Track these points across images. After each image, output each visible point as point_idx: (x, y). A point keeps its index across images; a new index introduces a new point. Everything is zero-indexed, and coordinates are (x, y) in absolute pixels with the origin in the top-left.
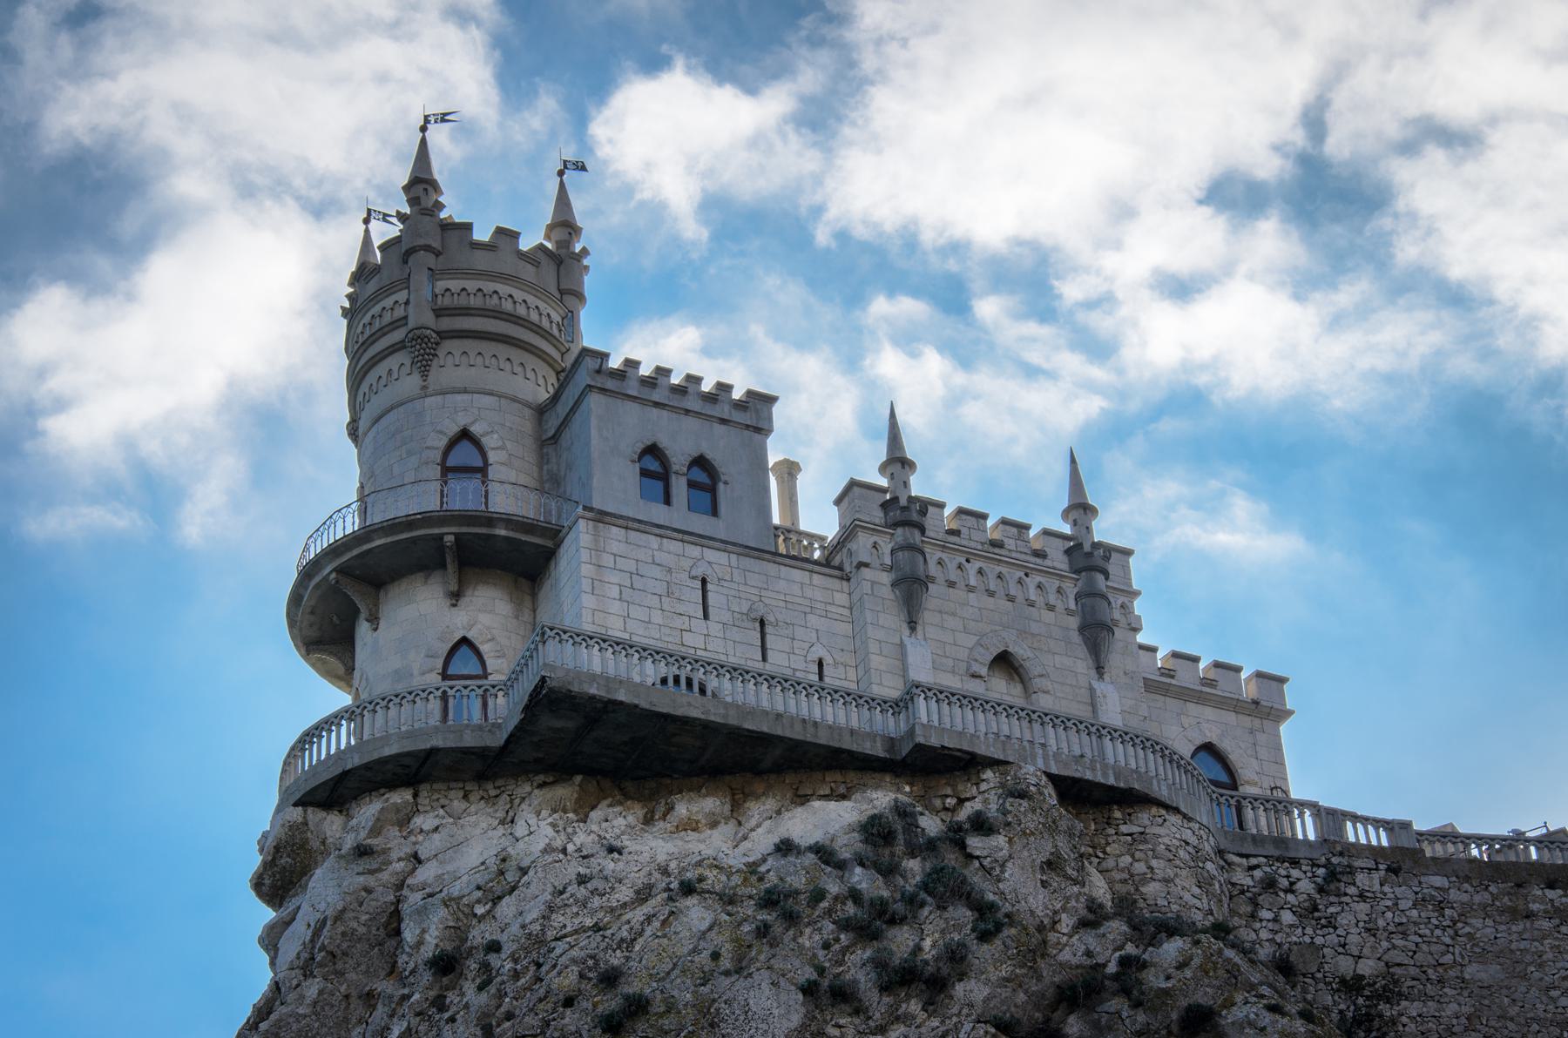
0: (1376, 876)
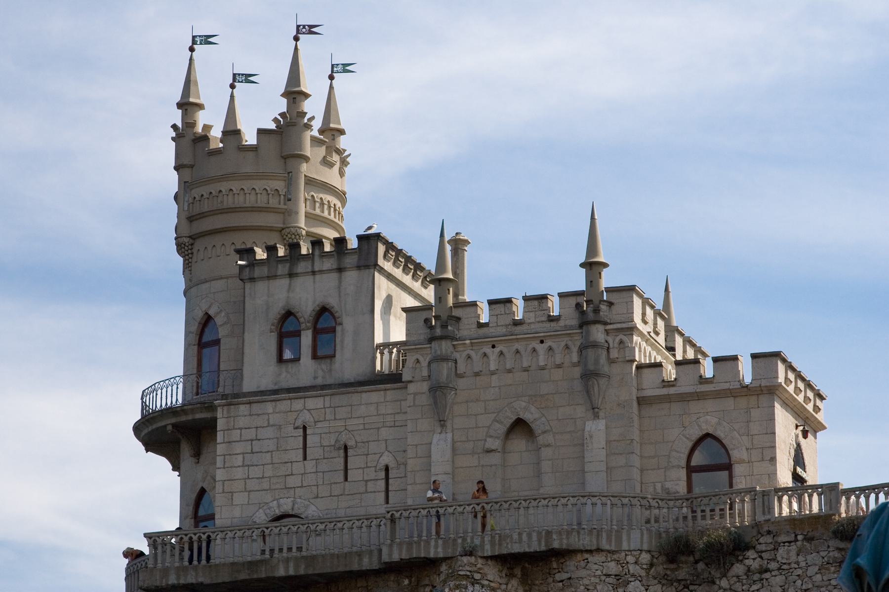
0: (793, 547)
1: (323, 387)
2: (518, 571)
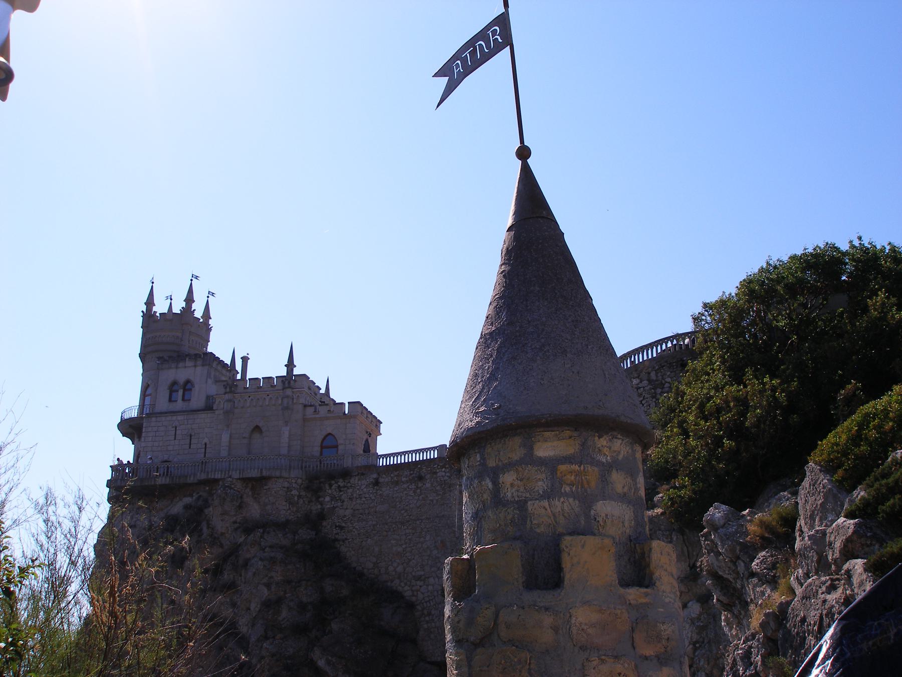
1: (184, 412)
2: (250, 485)
